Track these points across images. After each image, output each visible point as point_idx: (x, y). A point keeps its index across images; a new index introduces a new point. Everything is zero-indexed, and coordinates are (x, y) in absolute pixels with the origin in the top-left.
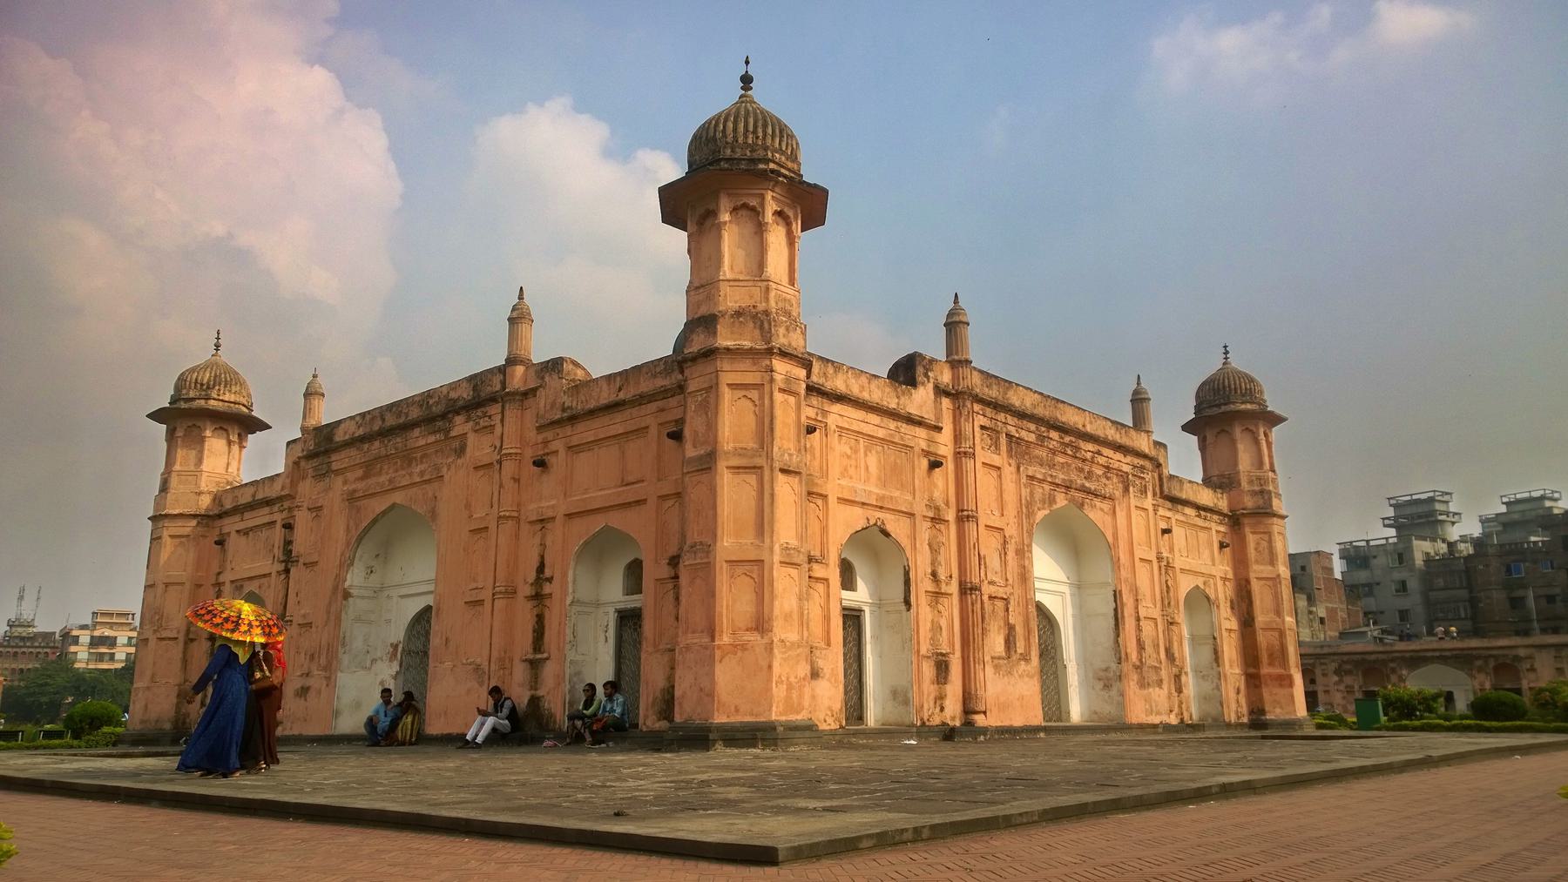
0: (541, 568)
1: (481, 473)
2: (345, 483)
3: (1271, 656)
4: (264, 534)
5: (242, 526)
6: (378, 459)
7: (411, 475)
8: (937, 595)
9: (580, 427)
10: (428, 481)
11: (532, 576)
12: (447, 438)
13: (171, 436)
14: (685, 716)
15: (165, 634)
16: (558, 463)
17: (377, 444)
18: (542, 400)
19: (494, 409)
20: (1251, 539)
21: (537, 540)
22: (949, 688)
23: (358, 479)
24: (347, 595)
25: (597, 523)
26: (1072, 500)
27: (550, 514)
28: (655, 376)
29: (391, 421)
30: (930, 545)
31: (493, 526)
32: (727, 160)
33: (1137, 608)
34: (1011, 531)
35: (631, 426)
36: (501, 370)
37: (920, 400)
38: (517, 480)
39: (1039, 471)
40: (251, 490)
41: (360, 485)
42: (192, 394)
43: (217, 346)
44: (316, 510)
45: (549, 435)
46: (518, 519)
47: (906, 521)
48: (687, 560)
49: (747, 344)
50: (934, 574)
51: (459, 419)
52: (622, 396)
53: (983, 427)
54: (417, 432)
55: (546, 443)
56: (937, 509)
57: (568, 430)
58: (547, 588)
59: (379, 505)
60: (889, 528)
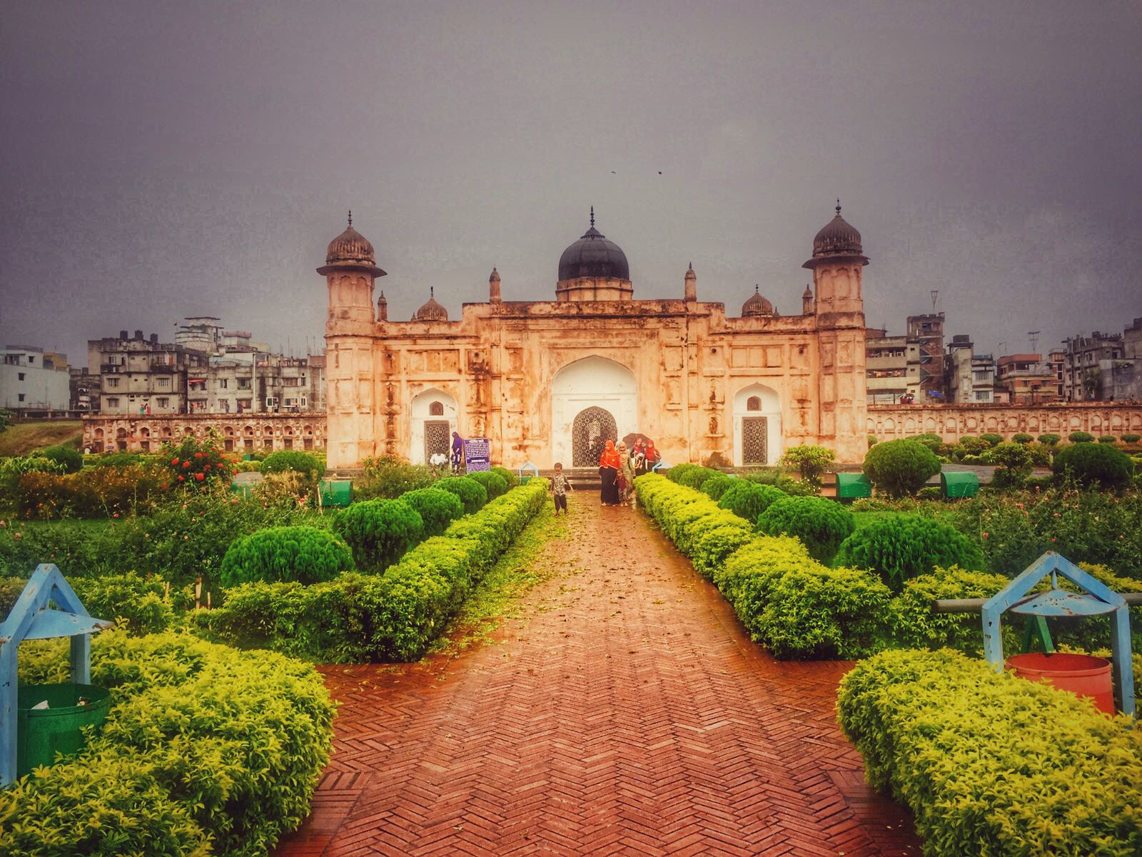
0: (713, 397)
5: (416, 348)
9: (738, 337)
11: (708, 401)
15: (364, 410)
25: (752, 381)
27: (720, 374)
28: (786, 324)
35: (772, 342)
42: (360, 256)
44: (515, 351)
45: (717, 338)
51: (649, 320)
52: (766, 328)
54: (614, 321)
55: (714, 341)
57: (730, 338)
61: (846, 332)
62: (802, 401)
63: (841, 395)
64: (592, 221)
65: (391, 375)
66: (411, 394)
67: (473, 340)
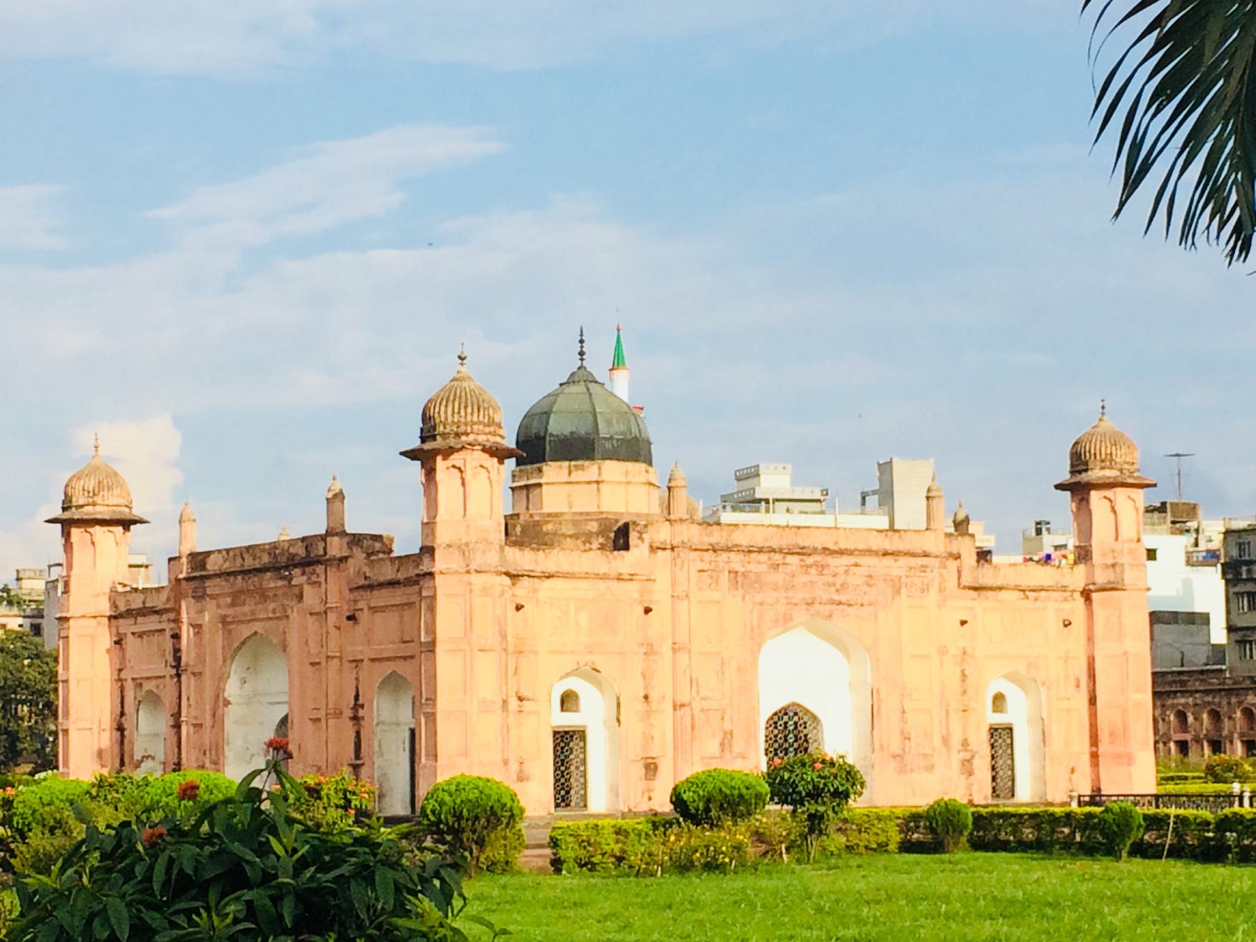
0: (357, 697)
3: (1111, 734)
5: (136, 629)
16: (364, 617)
19: (320, 569)
24: (227, 703)
29: (249, 563)
30: (643, 675)
31: (323, 662)
33: (902, 701)
40: (141, 597)
41: (230, 611)
42: (81, 503)
49: (454, 566)
51: (297, 571)
55: (356, 601)
58: (361, 713)
59: (246, 631)
64: (582, 354)
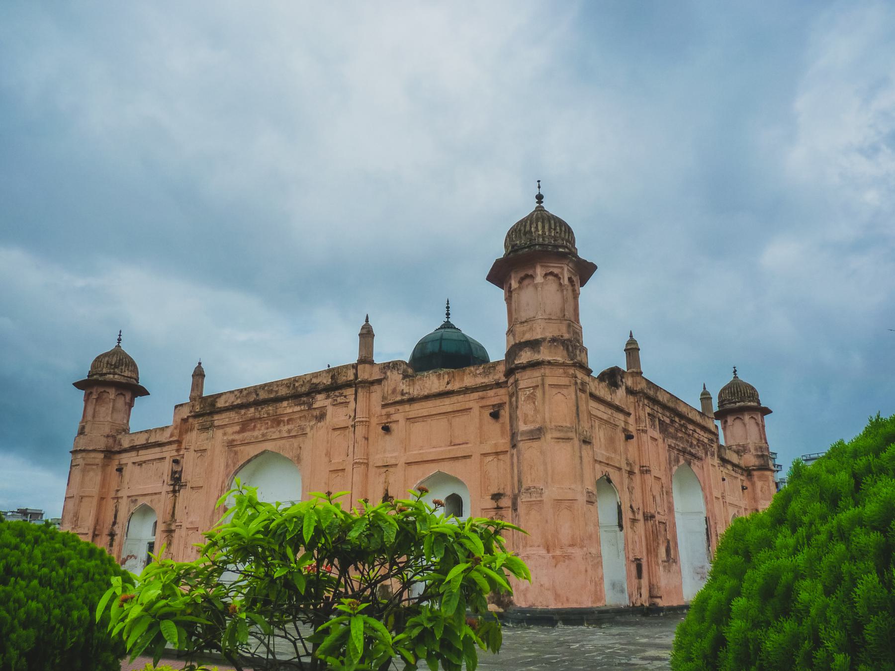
1: (338, 432)
2: (225, 434)
4: (156, 465)
5: (138, 459)
6: (252, 420)
7: (280, 431)
8: (634, 521)
9: (416, 406)
10: (295, 436)
12: (310, 408)
13: (87, 399)
14: (529, 603)
17: (252, 410)
18: (388, 386)
19: (350, 392)
20: (759, 484)
21: (382, 479)
22: (642, 581)
23: (234, 433)
25: (433, 469)
26: (686, 460)
27: (393, 462)
28: (475, 376)
29: (263, 395)
31: (349, 468)
32: (540, 245)
34: (664, 480)
36: (355, 367)
37: (620, 396)
38: (367, 439)
39: (672, 442)
41: (236, 437)
42: (104, 371)
43: (119, 340)
45: (391, 410)
46: (367, 464)
47: (617, 472)
48: (524, 498)
49: (560, 359)
50: (631, 507)
51: (320, 397)
52: (450, 387)
53: (649, 414)
54: (285, 404)
55: (388, 415)
56: (631, 464)
57: (407, 407)
59: (253, 451)
60: (611, 477)
61: (528, 373)
62: (496, 497)
63: (527, 482)
64: (448, 314)
65: (118, 491)
66: (129, 511)
67: (175, 446)
